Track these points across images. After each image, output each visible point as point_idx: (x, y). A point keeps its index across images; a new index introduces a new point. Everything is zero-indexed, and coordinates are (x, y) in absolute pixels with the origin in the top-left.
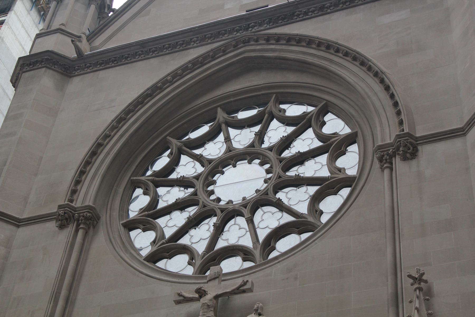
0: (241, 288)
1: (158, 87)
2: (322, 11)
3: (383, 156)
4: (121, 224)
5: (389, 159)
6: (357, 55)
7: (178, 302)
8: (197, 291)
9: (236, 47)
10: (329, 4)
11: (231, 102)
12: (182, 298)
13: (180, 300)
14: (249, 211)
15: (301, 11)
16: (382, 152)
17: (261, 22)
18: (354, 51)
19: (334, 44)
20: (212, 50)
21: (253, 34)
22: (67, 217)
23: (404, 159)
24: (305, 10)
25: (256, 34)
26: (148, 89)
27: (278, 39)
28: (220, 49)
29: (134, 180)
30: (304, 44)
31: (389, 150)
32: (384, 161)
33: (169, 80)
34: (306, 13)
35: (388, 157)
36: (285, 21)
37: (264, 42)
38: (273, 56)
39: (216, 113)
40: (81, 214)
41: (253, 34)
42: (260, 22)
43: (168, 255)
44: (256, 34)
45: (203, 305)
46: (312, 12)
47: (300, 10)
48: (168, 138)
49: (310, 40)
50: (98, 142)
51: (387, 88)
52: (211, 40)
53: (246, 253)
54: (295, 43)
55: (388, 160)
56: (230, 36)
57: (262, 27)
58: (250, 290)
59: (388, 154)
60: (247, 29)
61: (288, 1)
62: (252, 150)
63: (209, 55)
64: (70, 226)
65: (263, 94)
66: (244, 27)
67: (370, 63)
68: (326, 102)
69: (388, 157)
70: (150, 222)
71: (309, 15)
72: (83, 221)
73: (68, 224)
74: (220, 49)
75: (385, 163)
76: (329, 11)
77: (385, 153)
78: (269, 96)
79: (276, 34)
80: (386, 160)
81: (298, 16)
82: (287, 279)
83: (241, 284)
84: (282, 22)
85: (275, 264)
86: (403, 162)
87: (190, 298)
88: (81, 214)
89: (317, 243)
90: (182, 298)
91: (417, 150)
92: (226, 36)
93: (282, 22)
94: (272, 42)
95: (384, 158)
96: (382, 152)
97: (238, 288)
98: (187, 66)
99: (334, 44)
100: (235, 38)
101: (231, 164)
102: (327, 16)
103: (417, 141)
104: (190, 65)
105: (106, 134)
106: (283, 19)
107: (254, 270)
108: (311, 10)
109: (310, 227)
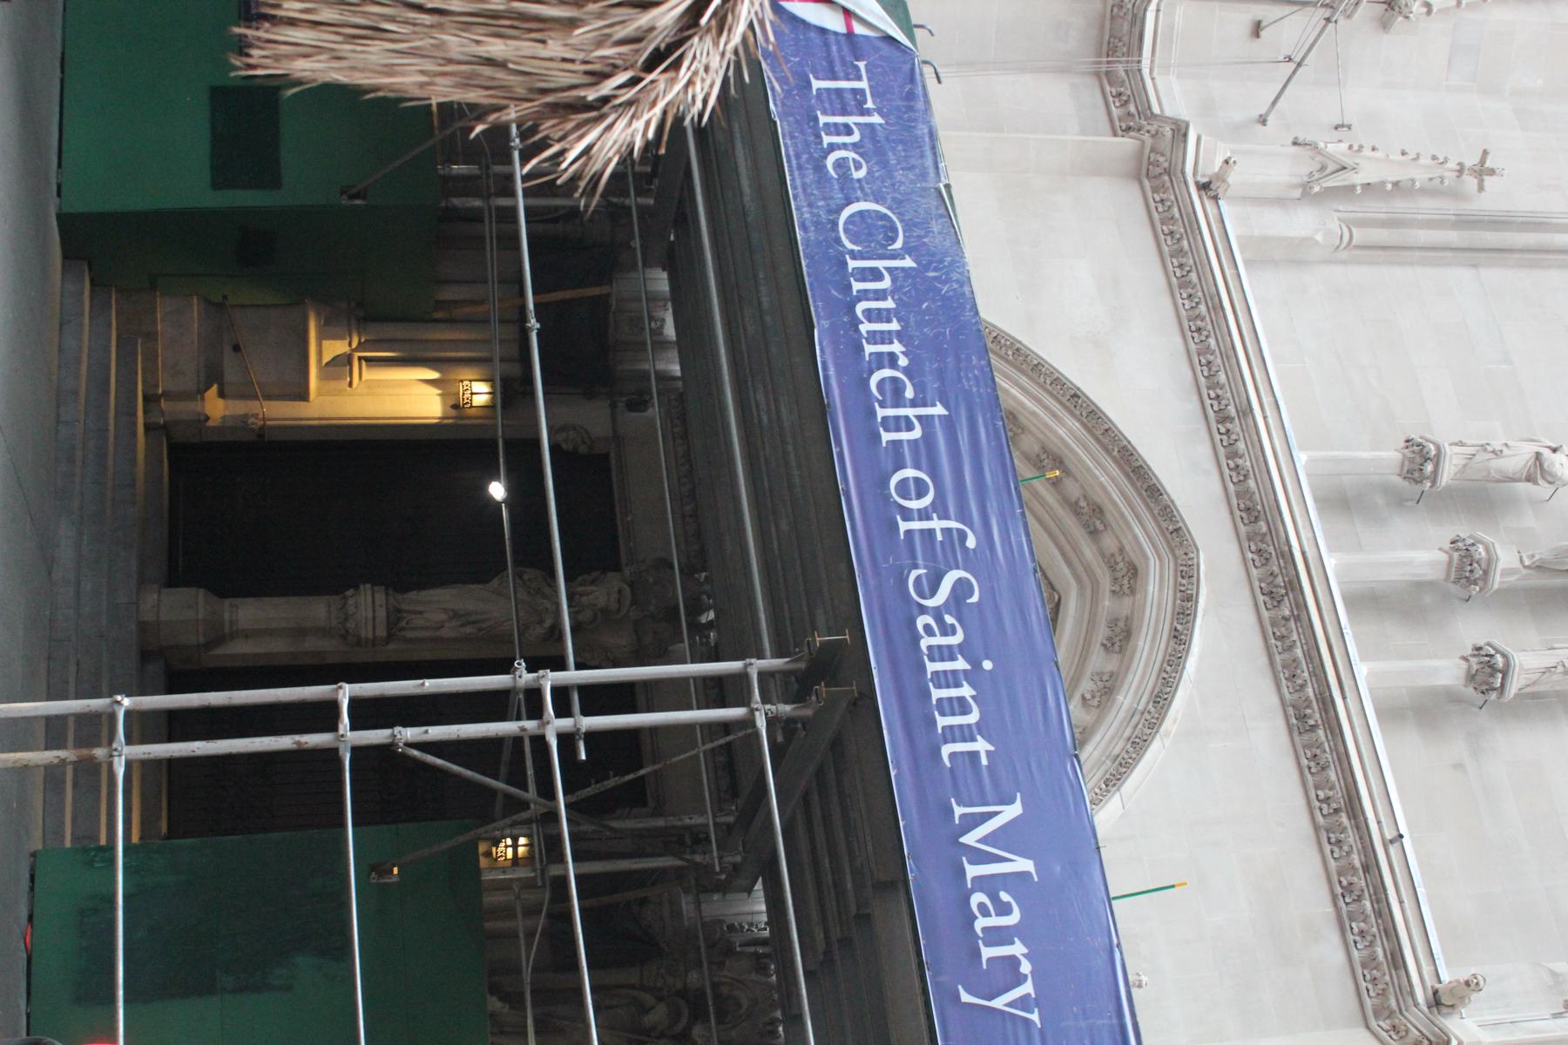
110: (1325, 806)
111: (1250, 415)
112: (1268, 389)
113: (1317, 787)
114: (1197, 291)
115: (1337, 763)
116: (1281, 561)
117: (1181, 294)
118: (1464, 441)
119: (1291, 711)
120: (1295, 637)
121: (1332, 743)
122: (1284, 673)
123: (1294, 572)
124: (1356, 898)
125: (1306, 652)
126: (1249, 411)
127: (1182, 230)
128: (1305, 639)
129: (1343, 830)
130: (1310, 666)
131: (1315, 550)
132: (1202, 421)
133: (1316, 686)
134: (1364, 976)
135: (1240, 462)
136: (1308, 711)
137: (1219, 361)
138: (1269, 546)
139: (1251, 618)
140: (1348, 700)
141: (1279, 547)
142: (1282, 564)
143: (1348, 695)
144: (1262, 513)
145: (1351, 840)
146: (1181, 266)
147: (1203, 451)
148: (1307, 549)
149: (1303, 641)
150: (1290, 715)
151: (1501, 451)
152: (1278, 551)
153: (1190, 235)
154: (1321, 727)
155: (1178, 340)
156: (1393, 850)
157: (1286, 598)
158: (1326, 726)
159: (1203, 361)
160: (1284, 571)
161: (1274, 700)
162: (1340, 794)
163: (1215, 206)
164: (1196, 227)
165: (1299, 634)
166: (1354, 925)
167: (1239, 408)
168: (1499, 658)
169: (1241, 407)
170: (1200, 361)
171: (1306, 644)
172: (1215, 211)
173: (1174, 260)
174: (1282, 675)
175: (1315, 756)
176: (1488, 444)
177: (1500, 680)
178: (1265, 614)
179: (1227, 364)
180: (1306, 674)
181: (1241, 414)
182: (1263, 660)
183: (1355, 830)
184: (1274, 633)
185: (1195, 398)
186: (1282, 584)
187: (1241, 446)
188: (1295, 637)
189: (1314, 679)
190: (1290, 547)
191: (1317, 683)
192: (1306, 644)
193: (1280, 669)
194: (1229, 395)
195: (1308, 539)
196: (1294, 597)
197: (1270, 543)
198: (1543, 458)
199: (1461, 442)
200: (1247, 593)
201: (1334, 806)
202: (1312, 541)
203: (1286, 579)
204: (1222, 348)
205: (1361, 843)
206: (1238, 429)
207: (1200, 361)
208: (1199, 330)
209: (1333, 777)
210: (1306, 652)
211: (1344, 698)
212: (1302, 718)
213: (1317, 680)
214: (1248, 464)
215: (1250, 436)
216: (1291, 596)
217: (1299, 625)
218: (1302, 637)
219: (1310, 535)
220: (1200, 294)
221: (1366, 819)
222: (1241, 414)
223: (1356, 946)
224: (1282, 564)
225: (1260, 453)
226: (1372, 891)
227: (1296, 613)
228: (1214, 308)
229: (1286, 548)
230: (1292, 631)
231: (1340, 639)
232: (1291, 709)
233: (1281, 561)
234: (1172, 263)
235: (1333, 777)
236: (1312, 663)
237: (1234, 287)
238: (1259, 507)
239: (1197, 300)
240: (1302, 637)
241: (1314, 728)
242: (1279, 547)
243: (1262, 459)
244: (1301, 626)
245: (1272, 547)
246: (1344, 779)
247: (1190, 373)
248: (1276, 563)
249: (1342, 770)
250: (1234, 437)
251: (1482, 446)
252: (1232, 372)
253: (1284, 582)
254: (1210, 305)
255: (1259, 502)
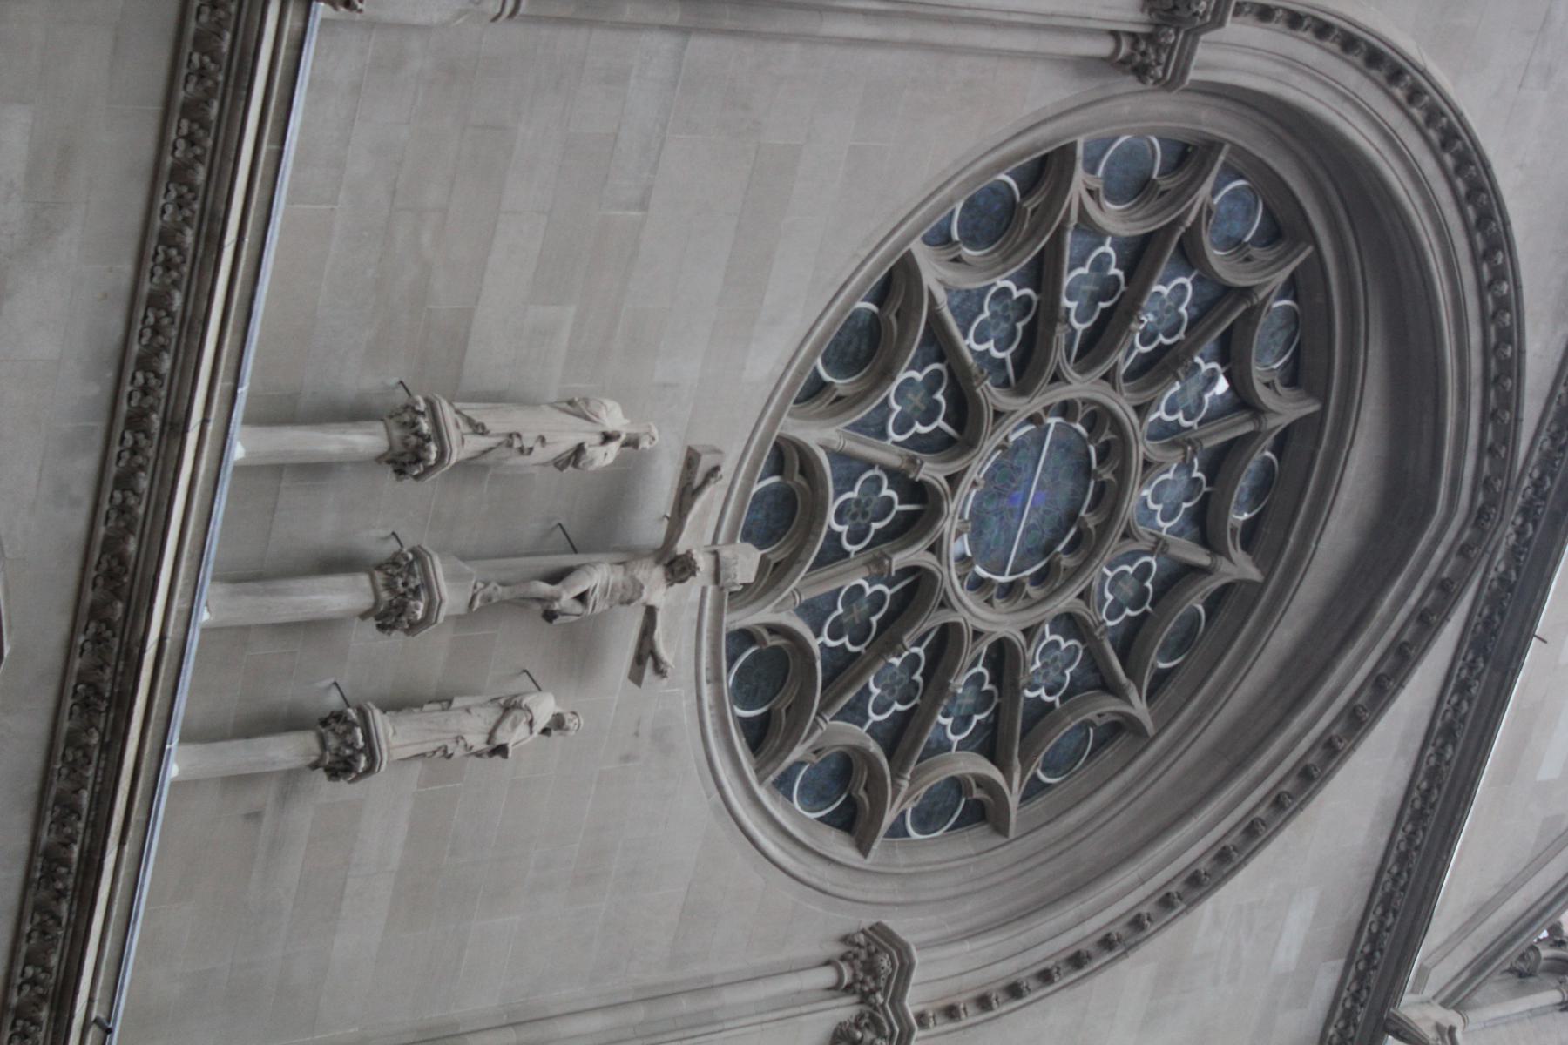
0: (650, 662)
1: (1495, 253)
2: (1441, 732)
3: (876, 978)
4: (1073, 145)
5: (861, 990)
6: (1231, 866)
7: (691, 460)
8: (690, 566)
9: (1482, 483)
10: (1448, 756)
11: (1317, 443)
12: (698, 480)
13: (694, 473)
14: (935, 483)
15: (1478, 677)
16: (890, 977)
17: (1518, 560)
18: (1244, 863)
19: (1302, 798)
20: (1517, 420)
21: (1490, 549)
22: (1177, 13)
23: (839, 1033)
24: (1473, 691)
25: (1487, 556)
26: (1506, 223)
27: (1427, 622)
28: (1505, 443)
29: (1219, 152)
30: (1361, 700)
31: (885, 996)
32: (861, 976)
33: (1498, 287)
34: (1463, 688)
35: (866, 989)
36: (1479, 627)
37: (1445, 575)
38: (1381, 602)
39: (1311, 393)
40: (1164, 57)
41: (1490, 549)
42: (1522, 558)
43: (887, 317)
44: (1487, 556)
45: (638, 588)
46: (1458, 704)
47: (1485, 677)
48: (1310, 249)
49: (1362, 723)
50: (1408, 73)
51: (1077, 960)
52: (1560, 397)
53: (778, 569)
54: (1382, 670)
55: (858, 986)
56: (1526, 482)
57: (1505, 557)
58: (636, 677)
59: (873, 992)
60: (1527, 511)
61: (1538, 637)
62: (1118, 530)
63: (1507, 408)
64: (1144, 17)
65: (1285, 541)
66: (1538, 506)
67: (1182, 907)
68: (1147, 736)
69: (866, 989)
70: (1034, 240)
71: (1407, 823)
72: (1138, 58)
73: (1151, 11)
74: (1505, 443)
75: (854, 975)
76: (1430, 751)
77: (882, 984)
78: (1267, 565)
79: (1445, 619)
80: (863, 982)
81: (1471, 666)
82: (637, 734)
83: (662, 662)
84: (1428, 763)
85: (788, 367)
86: (833, 1028)
87: (690, 506)
88: (1164, 57)
89: (709, 797)
90: (698, 480)
91: (856, 1020)
92: (1547, 445)
93: (1480, 615)
94: (1432, 595)
95: (869, 978)
96: (890, 977)
97: (653, 654)
98: (1510, 342)
99: (1302, 798)
100: (1510, 493)
101: (1104, 466)
102: (1415, 745)
103: (1187, 33)
104: (1508, 352)
105: (1426, 93)
106: (1488, 622)
107: (747, 470)
108: (1530, 527)
109: (778, 742)
110: (27, 988)
111: (179, 439)
112: (241, 327)
113: (26, 964)
114: (195, 199)
115: (68, 942)
116: (121, 663)
117: (168, 191)
118: (488, 426)
119: (39, 863)
120: (91, 772)
121: (73, 917)
122: (53, 812)
123: (130, 687)
124: (103, 627)
125: (96, 795)
126: (181, 429)
127: (221, 78)
128: (103, 776)
129: (36, 1022)
130: (93, 813)
131: (181, 629)
132: (105, 415)
133: (87, 841)
134: (123, 438)
135: (132, 501)
136: (63, 870)
137: (174, 333)
138: (114, 636)
139: (41, 726)
140: (127, 848)
141: (128, 643)
142: (121, 668)
143: (131, 833)
144: (128, 586)
145: (41, 1035)
146: (191, 141)
147: (87, 464)
148: (170, 633)
149: (99, 780)
150: (36, 867)
151: (531, 449)
152: (124, 648)
153: (230, 90)
154: (69, 898)
155: (127, 267)
156: (93, 1032)
157: (103, 715)
158: (77, 894)
159: (151, 320)
160: (119, 678)
161: (22, 842)
162: (52, 981)
163: (302, 13)
164: (246, 84)
165: (97, 768)
166: (196, 57)
167: (169, 420)
168: (433, 448)
169: (172, 417)
170: (146, 317)
171: (101, 783)
172: (298, 24)
173: (185, 123)
174: (49, 813)
175: (26, 1037)
176: (519, 435)
177: (360, 736)
178: (66, 725)
179: (183, 340)
180: (81, 825)
181: (167, 428)
182: (33, 786)
183: (52, 1024)
184: (64, 755)
185: (110, 375)
186: (107, 695)
187: (143, 483)
188: (91, 772)
189: (89, 831)
190: (143, 651)
191: (91, 837)
192: (121, 685)
193: (50, 803)
194: (163, 393)
195: (179, 612)
196: (115, 718)
197: (118, 632)
198: (583, 456)
199: (483, 427)
200: (50, 691)
201: (40, 990)
202: (184, 616)
203: (116, 690)
204: (189, 313)
205: (53, 1039)
206: (151, 452)
207: (146, 317)
208: (202, 73)
209: (54, 960)
210: (96, 795)
211: (122, 842)
212: (50, 876)
213: (92, 834)
214: (141, 510)
215: (164, 465)
216: (112, 715)
217: (103, 756)
218: (100, 773)
219: (186, 606)
220: (197, 206)
221: (71, 1017)
222: (167, 428)
223: (197, 18)
224: (121, 668)
225: (166, 501)
226: (102, 763)
227: (107, 739)
228: (208, 239)
229: (137, 651)
230: (90, 763)
231: (155, 759)
232: (40, 859)
233: (121, 663)
234: (179, 128)
235: (54, 960)
236: (97, 809)
237: (154, 735)
238: (126, 580)
239: (187, 213)
240: (100, 773)
241: (60, 895)
242: (128, 643)
243: (164, 510)
244: (106, 759)
245: (117, 640)
246: (68, 961)
247: (119, 332)
248: (113, 663)
249: (71, 949)
250: (140, 459)
251: (511, 435)
252: (186, 354)
253: (112, 691)
254: (204, 229)
255: (131, 567)
